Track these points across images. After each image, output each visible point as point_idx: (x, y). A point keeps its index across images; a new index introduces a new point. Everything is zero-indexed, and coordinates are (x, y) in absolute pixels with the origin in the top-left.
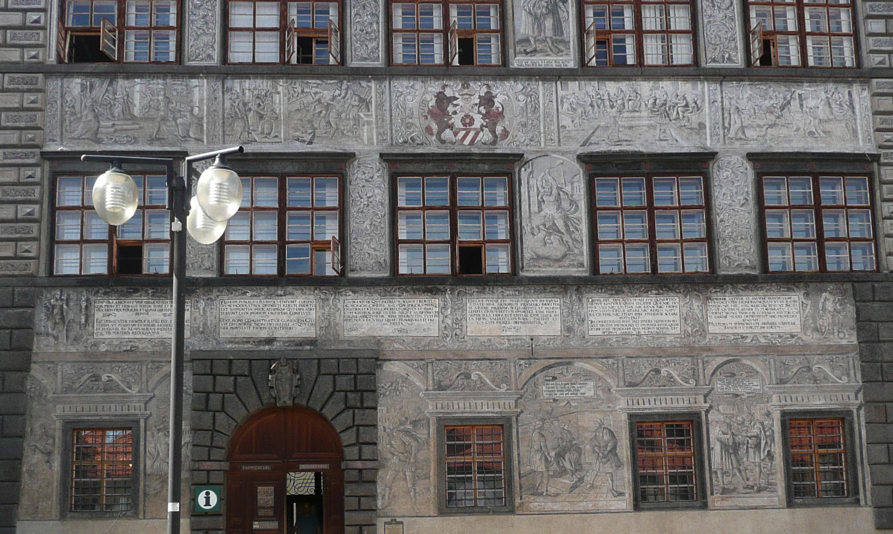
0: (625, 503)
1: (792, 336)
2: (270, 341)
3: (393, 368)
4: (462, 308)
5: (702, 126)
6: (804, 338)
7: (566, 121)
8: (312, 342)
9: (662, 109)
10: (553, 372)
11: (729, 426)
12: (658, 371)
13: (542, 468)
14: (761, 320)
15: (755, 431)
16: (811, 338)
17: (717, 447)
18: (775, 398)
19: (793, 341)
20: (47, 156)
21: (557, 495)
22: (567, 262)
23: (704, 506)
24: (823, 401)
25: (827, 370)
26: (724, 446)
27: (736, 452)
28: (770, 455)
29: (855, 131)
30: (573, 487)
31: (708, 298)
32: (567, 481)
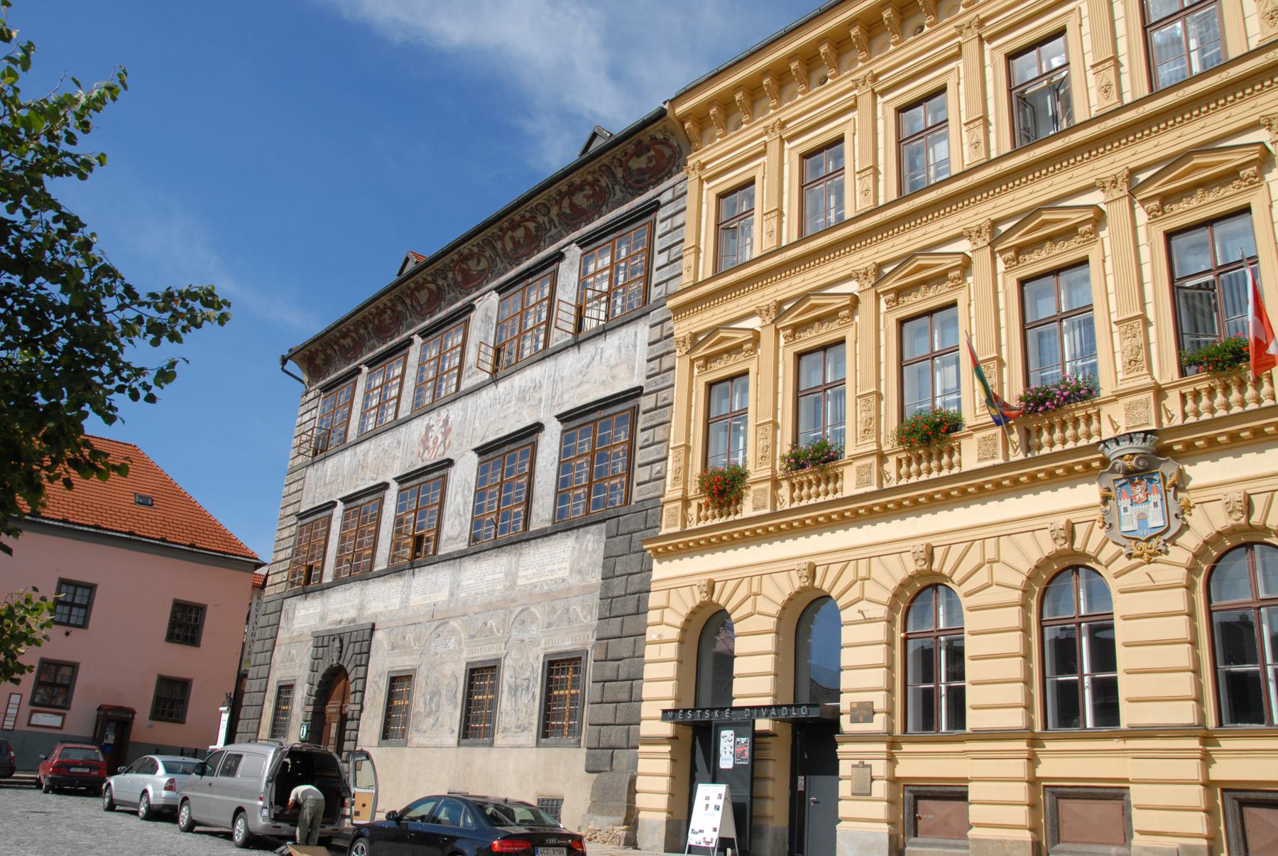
0: (453, 740)
1: (563, 580)
2: (341, 622)
3: (378, 635)
4: (410, 587)
5: (540, 400)
6: (571, 581)
7: (477, 425)
8: (354, 620)
9: (522, 397)
10: (440, 630)
11: (515, 670)
12: (485, 624)
13: (422, 710)
14: (548, 568)
15: (528, 674)
16: (575, 580)
17: (506, 688)
18: (543, 641)
19: (562, 586)
20: (301, 516)
21: (425, 732)
22: (459, 539)
23: (491, 745)
24: (570, 643)
25: (578, 610)
26: (510, 687)
27: (516, 692)
28: (534, 695)
29: (633, 368)
30: (434, 725)
31: (521, 554)
32: (431, 720)
